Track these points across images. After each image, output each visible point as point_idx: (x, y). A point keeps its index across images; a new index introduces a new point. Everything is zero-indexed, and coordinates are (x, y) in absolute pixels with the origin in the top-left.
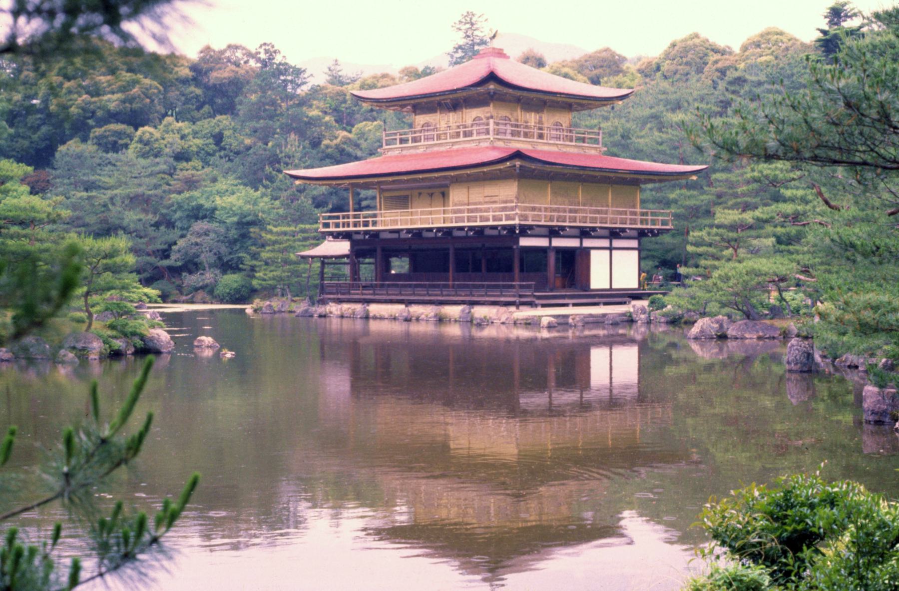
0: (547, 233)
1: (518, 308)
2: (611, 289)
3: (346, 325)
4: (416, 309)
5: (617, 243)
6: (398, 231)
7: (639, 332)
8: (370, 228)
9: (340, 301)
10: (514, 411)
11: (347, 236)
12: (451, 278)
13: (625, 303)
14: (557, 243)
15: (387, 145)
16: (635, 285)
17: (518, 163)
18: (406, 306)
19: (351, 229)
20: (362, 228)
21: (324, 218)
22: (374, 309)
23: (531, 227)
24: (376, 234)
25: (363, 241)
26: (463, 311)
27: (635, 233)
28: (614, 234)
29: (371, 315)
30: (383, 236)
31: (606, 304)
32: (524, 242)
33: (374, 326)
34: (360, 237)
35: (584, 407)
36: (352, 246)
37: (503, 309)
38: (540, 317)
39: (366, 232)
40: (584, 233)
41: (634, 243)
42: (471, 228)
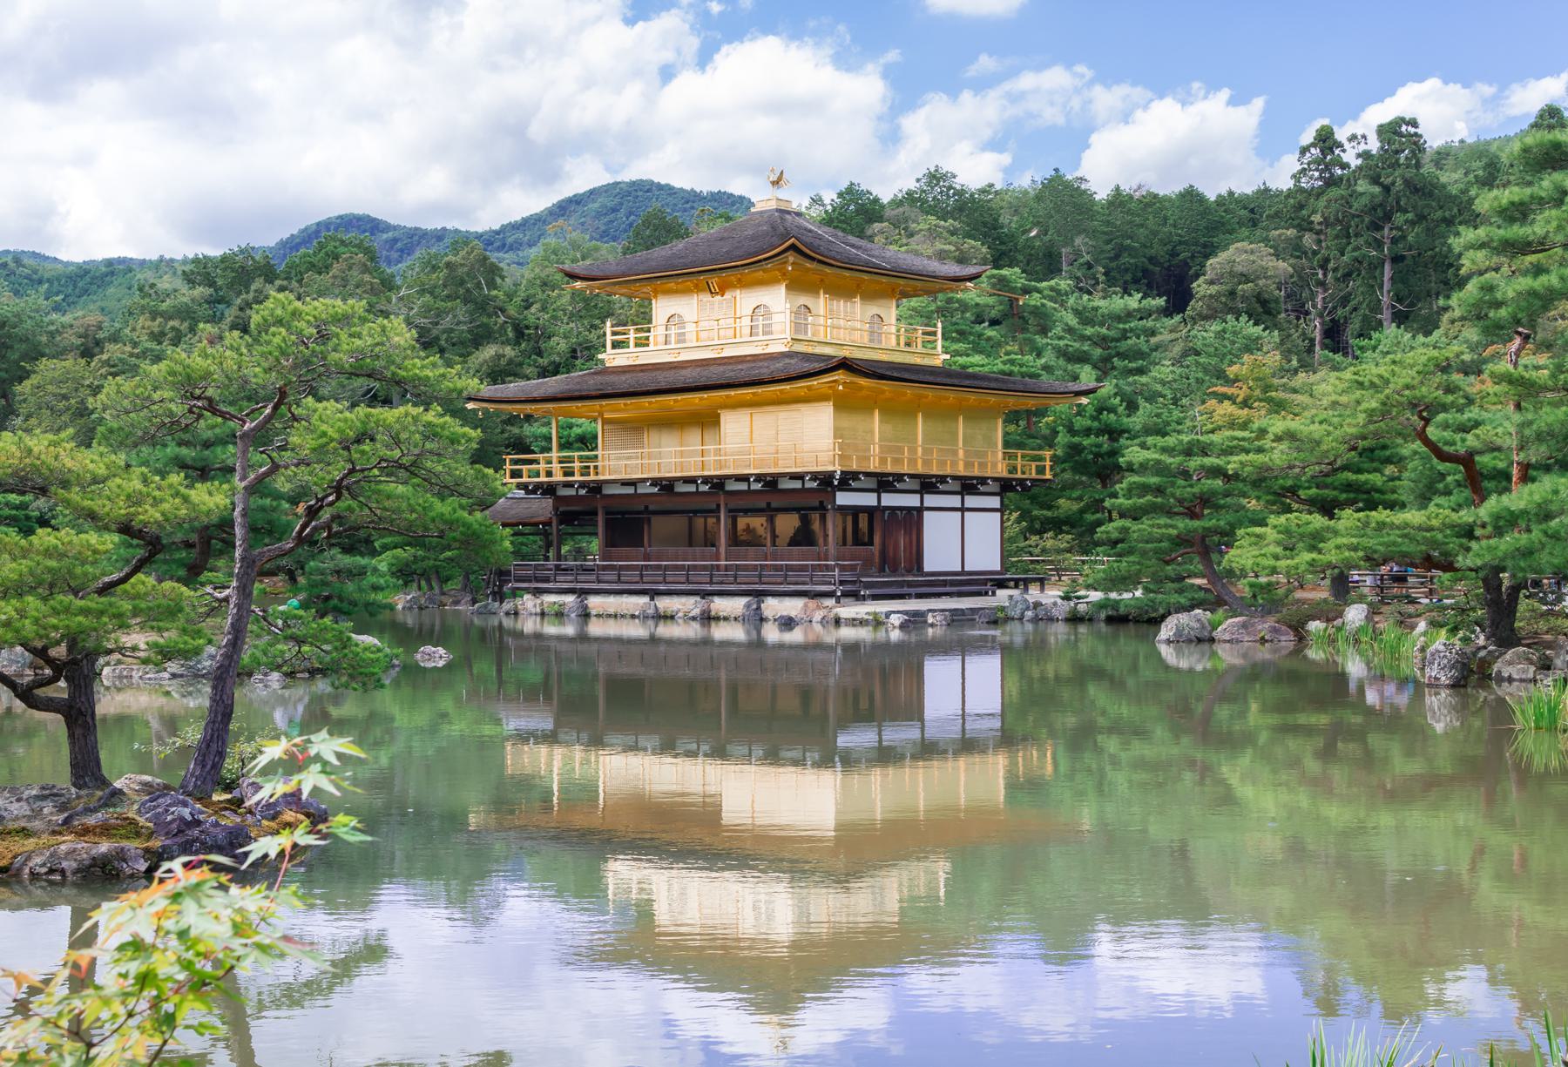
0: (874, 485)
1: (838, 602)
2: (963, 573)
3: (551, 629)
4: (665, 604)
5: (971, 501)
6: (632, 483)
7: (1017, 634)
8: (592, 477)
9: (537, 592)
11: (549, 490)
12: (723, 555)
13: (986, 594)
14: (889, 500)
15: (614, 347)
18: (652, 599)
19: (558, 477)
20: (577, 478)
21: (516, 462)
22: (594, 602)
23: (854, 475)
24: (596, 488)
25: (577, 499)
26: (748, 606)
27: (993, 486)
28: (969, 486)
29: (594, 612)
30: (608, 491)
31: (960, 594)
32: (843, 499)
33: (596, 628)
34: (571, 492)
36: (556, 508)
37: (812, 604)
38: (888, 615)
39: (583, 485)
41: (995, 502)
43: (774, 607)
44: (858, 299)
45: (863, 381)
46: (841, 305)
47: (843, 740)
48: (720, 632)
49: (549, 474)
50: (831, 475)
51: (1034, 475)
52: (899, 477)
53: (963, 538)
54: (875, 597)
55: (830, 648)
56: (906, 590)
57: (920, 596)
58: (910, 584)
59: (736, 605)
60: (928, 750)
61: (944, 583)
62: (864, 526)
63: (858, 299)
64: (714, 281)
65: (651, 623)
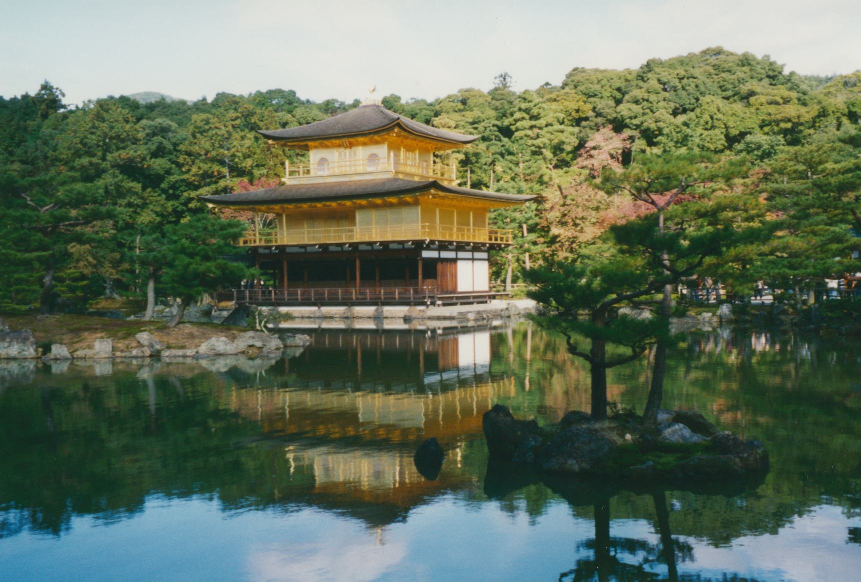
1: (428, 306)
4: (326, 310)
5: (478, 255)
10: (422, 390)
13: (486, 302)
14: (445, 255)
16: (487, 289)
17: (433, 191)
20: (274, 244)
24: (282, 249)
26: (377, 310)
28: (477, 248)
30: (288, 250)
32: (426, 254)
35: (463, 383)
37: (413, 308)
40: (461, 247)
41: (485, 255)
42: (382, 243)
43: (388, 310)
44: (417, 152)
45: (441, 194)
46: (410, 155)
47: (428, 380)
48: (359, 325)
49: (255, 242)
50: (423, 242)
51: (505, 242)
52: (451, 243)
53: (472, 275)
54: (444, 305)
55: (424, 332)
56: (455, 301)
57: (462, 304)
58: (458, 298)
59: (370, 310)
60: (463, 383)
61: (469, 298)
62: (432, 269)
63: (417, 152)
64: (346, 141)
65: (318, 321)
